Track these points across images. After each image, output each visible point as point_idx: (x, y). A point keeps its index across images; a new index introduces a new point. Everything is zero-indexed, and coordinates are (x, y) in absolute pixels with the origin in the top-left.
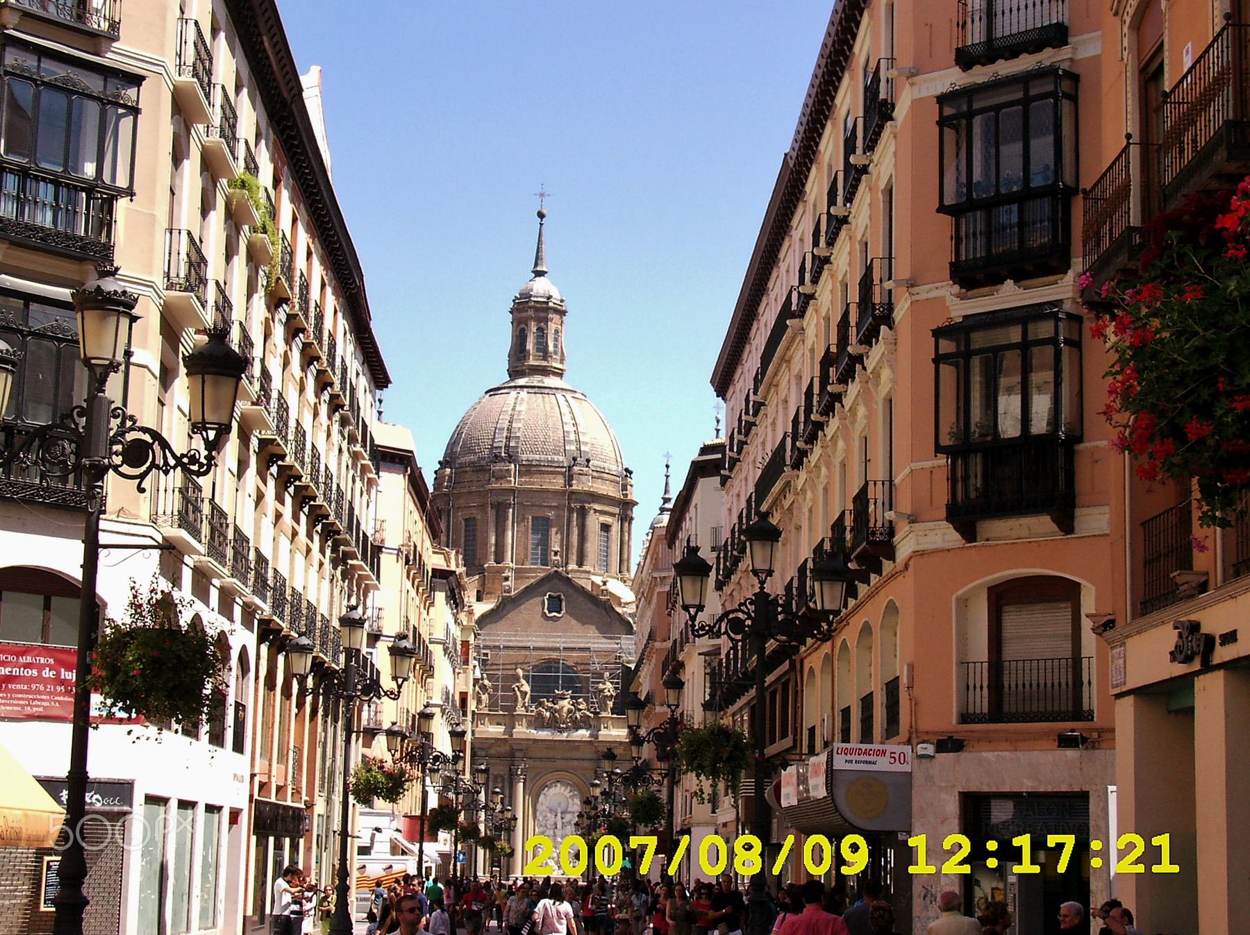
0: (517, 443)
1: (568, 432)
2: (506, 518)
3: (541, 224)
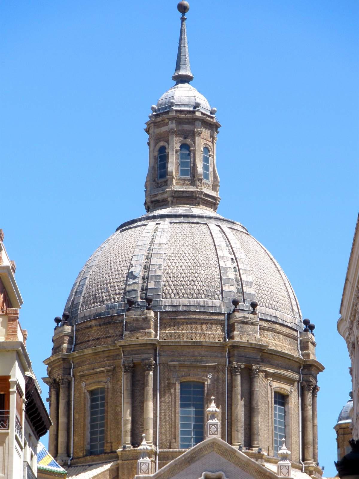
0: (158, 283)
1: (226, 269)
2: (144, 385)
3: (183, 20)
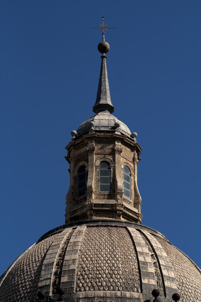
1: (145, 263)
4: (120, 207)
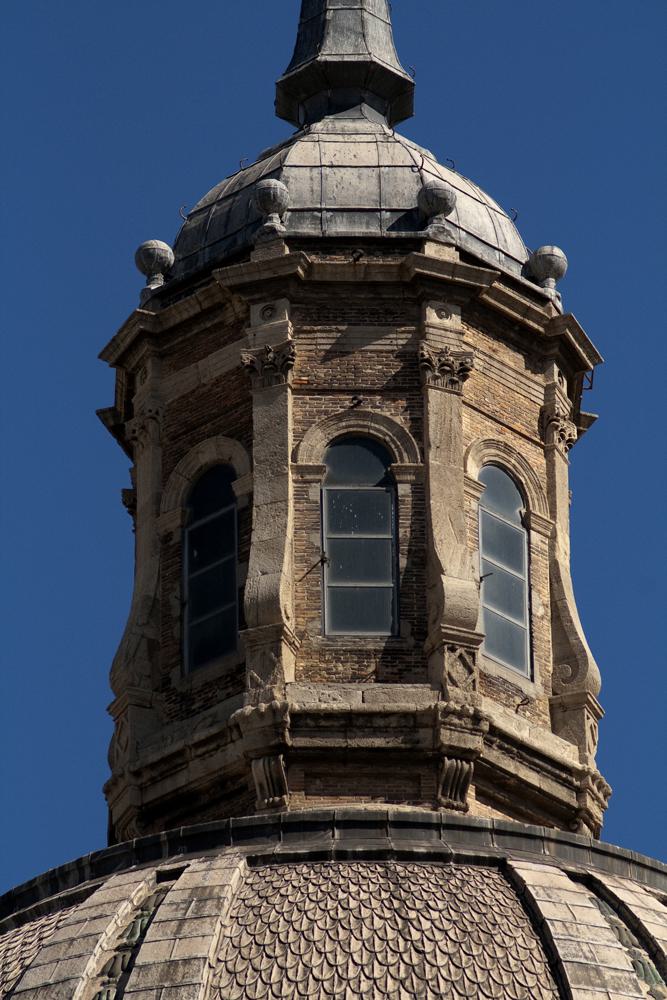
4: (461, 729)
